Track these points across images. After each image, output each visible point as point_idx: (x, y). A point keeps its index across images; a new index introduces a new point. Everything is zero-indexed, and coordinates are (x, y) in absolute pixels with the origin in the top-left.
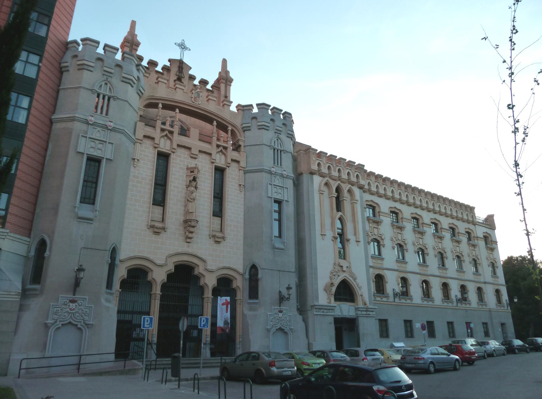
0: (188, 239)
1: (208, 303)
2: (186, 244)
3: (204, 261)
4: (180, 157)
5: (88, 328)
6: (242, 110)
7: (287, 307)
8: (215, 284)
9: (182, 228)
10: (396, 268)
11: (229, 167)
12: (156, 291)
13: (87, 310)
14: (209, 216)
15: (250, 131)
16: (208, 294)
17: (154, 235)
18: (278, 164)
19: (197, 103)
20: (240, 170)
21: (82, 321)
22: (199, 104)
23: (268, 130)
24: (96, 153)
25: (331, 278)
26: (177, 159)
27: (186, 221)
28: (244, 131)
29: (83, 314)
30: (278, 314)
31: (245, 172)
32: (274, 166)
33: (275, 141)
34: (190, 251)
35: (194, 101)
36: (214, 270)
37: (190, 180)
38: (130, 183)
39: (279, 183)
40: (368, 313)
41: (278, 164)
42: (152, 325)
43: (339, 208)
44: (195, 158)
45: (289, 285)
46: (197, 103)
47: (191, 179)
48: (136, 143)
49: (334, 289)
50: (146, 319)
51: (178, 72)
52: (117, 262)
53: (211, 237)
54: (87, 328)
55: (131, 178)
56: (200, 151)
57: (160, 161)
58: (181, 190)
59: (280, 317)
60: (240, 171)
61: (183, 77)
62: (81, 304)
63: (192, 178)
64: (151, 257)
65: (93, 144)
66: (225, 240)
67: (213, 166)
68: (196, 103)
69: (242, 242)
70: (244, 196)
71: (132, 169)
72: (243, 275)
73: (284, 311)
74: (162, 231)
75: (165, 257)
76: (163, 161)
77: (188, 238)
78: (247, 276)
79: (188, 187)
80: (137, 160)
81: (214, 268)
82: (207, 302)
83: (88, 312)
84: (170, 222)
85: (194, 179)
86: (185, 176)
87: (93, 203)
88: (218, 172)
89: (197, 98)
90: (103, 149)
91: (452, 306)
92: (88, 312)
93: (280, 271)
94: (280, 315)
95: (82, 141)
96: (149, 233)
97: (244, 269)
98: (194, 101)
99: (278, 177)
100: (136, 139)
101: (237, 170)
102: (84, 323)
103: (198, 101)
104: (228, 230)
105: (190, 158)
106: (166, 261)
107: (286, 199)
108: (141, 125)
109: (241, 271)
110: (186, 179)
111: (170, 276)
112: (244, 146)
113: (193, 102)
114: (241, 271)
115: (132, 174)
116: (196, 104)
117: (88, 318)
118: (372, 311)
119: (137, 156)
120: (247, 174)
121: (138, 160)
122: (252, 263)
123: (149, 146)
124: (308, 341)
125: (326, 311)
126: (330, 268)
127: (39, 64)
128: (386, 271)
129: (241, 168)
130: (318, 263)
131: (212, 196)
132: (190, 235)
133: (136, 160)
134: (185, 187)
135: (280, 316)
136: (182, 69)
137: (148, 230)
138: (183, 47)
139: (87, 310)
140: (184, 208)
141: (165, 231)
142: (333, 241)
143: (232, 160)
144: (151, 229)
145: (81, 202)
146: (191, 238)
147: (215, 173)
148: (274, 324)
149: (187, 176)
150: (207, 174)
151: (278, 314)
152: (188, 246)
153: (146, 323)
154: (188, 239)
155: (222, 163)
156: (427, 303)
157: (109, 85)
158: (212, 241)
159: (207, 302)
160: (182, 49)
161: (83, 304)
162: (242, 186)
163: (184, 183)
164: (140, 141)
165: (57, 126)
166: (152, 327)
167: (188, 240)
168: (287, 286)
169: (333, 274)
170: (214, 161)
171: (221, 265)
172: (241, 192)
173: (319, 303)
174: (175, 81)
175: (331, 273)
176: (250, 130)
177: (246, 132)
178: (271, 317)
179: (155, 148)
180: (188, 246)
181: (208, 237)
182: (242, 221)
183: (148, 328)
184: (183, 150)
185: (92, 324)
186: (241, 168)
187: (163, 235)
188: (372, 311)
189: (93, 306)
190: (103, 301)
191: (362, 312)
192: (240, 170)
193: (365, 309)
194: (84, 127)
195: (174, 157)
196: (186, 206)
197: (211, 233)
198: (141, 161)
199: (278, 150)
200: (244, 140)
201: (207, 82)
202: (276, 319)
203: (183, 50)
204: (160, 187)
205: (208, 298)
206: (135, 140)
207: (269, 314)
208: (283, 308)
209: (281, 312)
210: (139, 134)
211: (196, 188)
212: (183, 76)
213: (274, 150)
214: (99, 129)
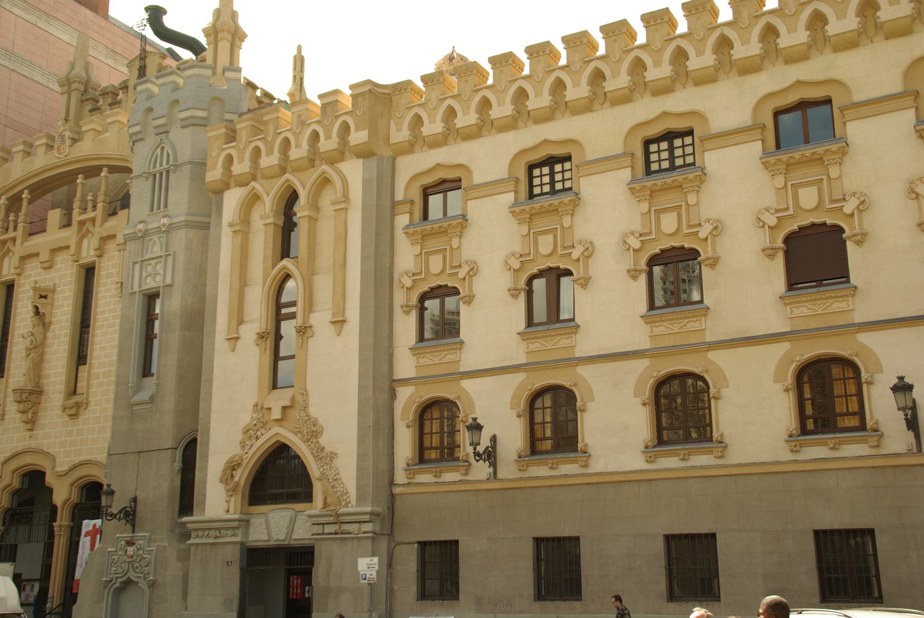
0: (31, 423)
7: (146, 531)
10: (522, 359)
16: (62, 521)
22: (66, 156)
23: (142, 139)
25: (243, 444)
34: (33, 444)
40: (346, 527)
43: (285, 252)
44: (50, 267)
49: (242, 476)
91: (682, 469)
93: (139, 452)
94: (131, 550)
99: (155, 238)
118: (359, 522)
125: (213, 533)
126: (246, 417)
128: (466, 384)
130: (213, 416)
142: (258, 345)
154: (31, 423)
156: (683, 464)
169: (250, 432)
171: (77, 460)
173: (204, 515)
175: (246, 431)
188: (359, 522)
191: (326, 526)
193: (331, 519)
209: (130, 543)
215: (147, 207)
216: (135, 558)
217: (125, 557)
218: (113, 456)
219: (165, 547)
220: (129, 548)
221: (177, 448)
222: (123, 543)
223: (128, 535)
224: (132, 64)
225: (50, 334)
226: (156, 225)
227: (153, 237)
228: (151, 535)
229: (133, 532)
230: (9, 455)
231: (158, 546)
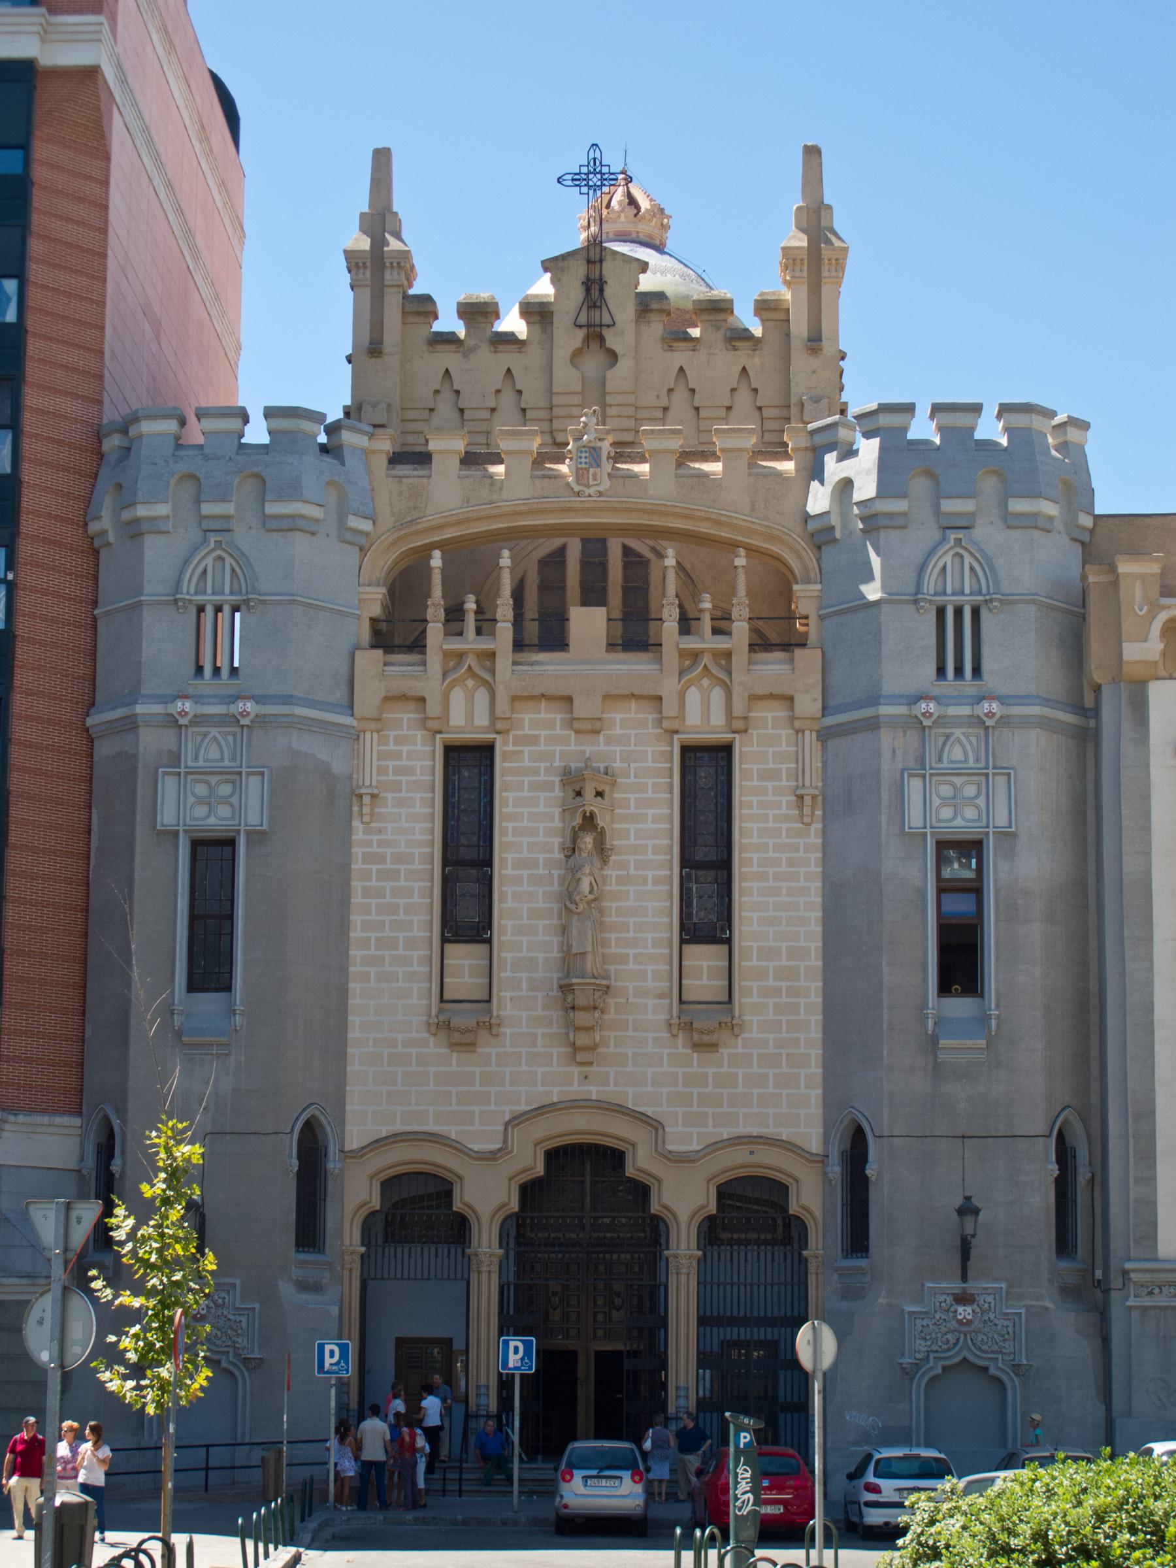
2: (576, 1070)
3: (654, 1125)
4: (534, 740)
5: (247, 1368)
7: (997, 1280)
9: (556, 1015)
12: (479, 1247)
13: (239, 1318)
18: (959, 671)
19: (592, 491)
21: (231, 1350)
22: (601, 494)
24: (216, 821)
26: (521, 752)
28: (819, 548)
29: (229, 1331)
30: (952, 1309)
31: (825, 736)
32: (936, 692)
33: (944, 568)
37: (574, 827)
38: (357, 885)
39: (966, 761)
41: (959, 671)
42: (347, 1365)
45: (968, 1199)
46: (592, 491)
47: (574, 824)
48: (362, 735)
50: (327, 1348)
51: (585, 308)
52: (333, 1163)
54: (245, 1372)
55: (357, 866)
56: (610, 698)
57: (466, 774)
58: (547, 872)
59: (960, 1322)
60: (800, 735)
61: (608, 326)
62: (220, 1301)
63: (578, 820)
65: (201, 790)
66: (737, 1036)
67: (671, 744)
68: (587, 492)
69: (816, 1034)
70: (820, 841)
72: (824, 1159)
73: (981, 1299)
74: (483, 1035)
75: (502, 1128)
76: (476, 771)
78: (835, 1170)
79: (571, 850)
80: (369, 797)
81: (695, 1146)
83: (244, 1324)
84: (511, 999)
85: (589, 821)
86: (557, 811)
87: (228, 988)
89: (591, 471)
90: (234, 800)
92: (244, 1324)
94: (964, 1312)
95: (168, 788)
96: (434, 1048)
97: (826, 1142)
98: (577, 488)
99: (958, 732)
101: (785, 733)
102: (236, 1355)
103: (595, 479)
104: (749, 995)
105: (573, 733)
106: (505, 1142)
107: (1001, 818)
108: (370, 660)
109: (815, 1145)
110: (561, 825)
111: (530, 1191)
112: (821, 618)
113: (578, 494)
114: (815, 1145)
115: (357, 851)
116: (590, 496)
117: (245, 1341)
119: (367, 783)
121: (373, 796)
122: (849, 1118)
123: (411, 732)
124: (1109, 1410)
127: (6, 575)
132: (582, 1040)
133: (366, 800)
134: (562, 856)
135: (960, 1317)
136: (601, 290)
138: (595, 180)
139: (239, 1318)
140: (560, 938)
143: (754, 698)
145: (192, 988)
146: (593, 1048)
148: (934, 1347)
149: (564, 810)
150: (650, 781)
151: (952, 1309)
152: (586, 1077)
153: (328, 1361)
155: (713, 723)
157: (229, 561)
158: (681, 1047)
160: (591, 192)
161: (226, 1301)
162: (808, 801)
163: (556, 841)
164: (372, 725)
165: (103, 749)
166: (347, 1371)
167: (580, 1057)
168: (958, 1201)
170: (675, 725)
171: (725, 1133)
172: (809, 824)
174: (577, 354)
178: (919, 1322)
180: (586, 1077)
182: (816, 945)
183: (337, 1373)
184: (544, 712)
185: (261, 1359)
187: (488, 1049)
189: (257, 1306)
190: (286, 1289)
192: (797, 732)
194: (168, 739)
195: (511, 748)
196: (564, 930)
197: (675, 1014)
198: (385, 795)
199: (959, 612)
201: (723, 306)
202: (944, 1330)
203: (599, 193)
204: (473, 872)
207: (909, 1312)
208: (975, 1285)
209: (963, 1299)
210: (369, 694)
211: (602, 850)
212: (607, 320)
213: (941, 612)
214: (214, 732)
215: (932, 670)
216: (976, 1323)
217: (954, 1322)
218: (895, 1139)
219: (1047, 1309)
220: (960, 1309)
221: (1049, 1136)
222: (949, 1299)
223: (956, 1285)
224: (561, 264)
225: (611, 873)
226: (966, 711)
227: (954, 730)
228: (1009, 1286)
229: (964, 1278)
230: (524, 1107)
231: (1028, 1308)
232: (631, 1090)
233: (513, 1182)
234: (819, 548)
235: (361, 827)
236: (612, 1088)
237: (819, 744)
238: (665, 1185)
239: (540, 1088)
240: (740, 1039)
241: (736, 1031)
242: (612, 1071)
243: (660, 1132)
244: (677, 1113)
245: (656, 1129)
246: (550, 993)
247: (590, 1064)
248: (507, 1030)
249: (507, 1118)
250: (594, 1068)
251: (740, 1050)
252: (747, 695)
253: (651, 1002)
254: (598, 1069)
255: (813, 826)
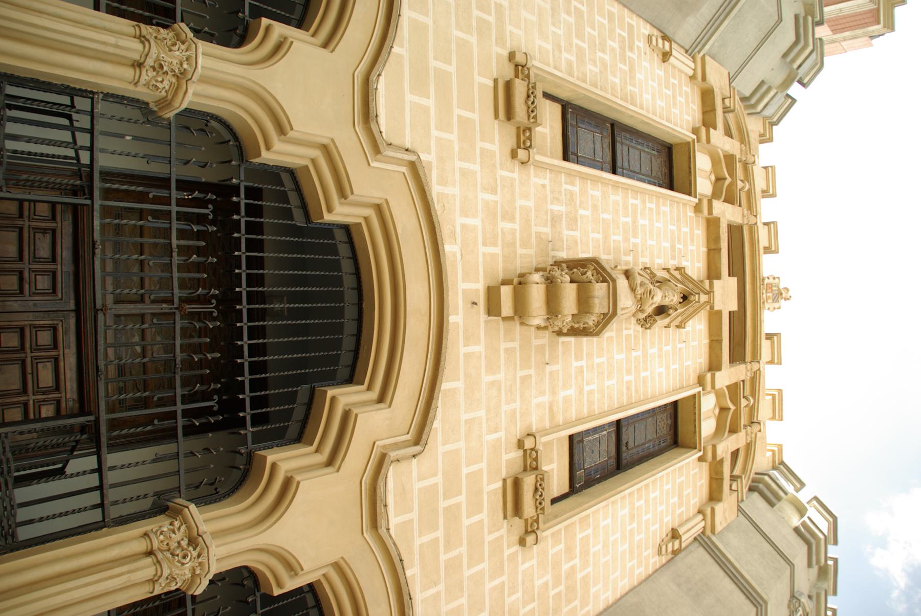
1: (149, 560)
2: (479, 287)
3: (420, 436)
6: (774, 461)
8: (291, 567)
11: (701, 459)
14: (560, 419)
15: (768, 507)
17: (491, 83)
20: (700, 512)
22: (763, 303)
27: (576, 266)
28: (751, 489)
34: (455, 319)
35: (767, 285)
36: (382, 523)
46: (764, 296)
53: (529, 444)
60: (700, 517)
64: (400, 49)
71: (646, 29)
75: (408, 146)
77: (520, 284)
82: (150, 553)
84: (544, 186)
88: (664, 422)
100: (703, 58)
120: (701, 550)
129: (708, 512)
131: (621, 408)
137: (505, 53)
141: (514, 155)
144: (508, 72)
146: (521, 310)
147: (653, 412)
159: (150, 553)
167: (506, 293)
171: (413, 572)
176: (772, 505)
177: (755, 495)
179: (695, 131)
181: (518, 431)
186: (708, 512)
192: (700, 512)
200: (745, 499)
205: (193, 542)
206: (699, 52)
232: (459, 385)
233: (317, 154)
234: (751, 489)
235: (647, 33)
236: (463, 350)
237: (692, 538)
238: (329, 477)
239: (460, 221)
240: (517, 548)
241: (530, 539)
242: (478, 349)
243: (417, 448)
244: (435, 474)
245: (417, 442)
246: (550, 245)
247: (493, 308)
248: (514, 173)
249: (422, 156)
250: (483, 316)
251: (507, 552)
252: (724, 456)
253: (545, 399)
254: (482, 325)
255: (657, 558)
